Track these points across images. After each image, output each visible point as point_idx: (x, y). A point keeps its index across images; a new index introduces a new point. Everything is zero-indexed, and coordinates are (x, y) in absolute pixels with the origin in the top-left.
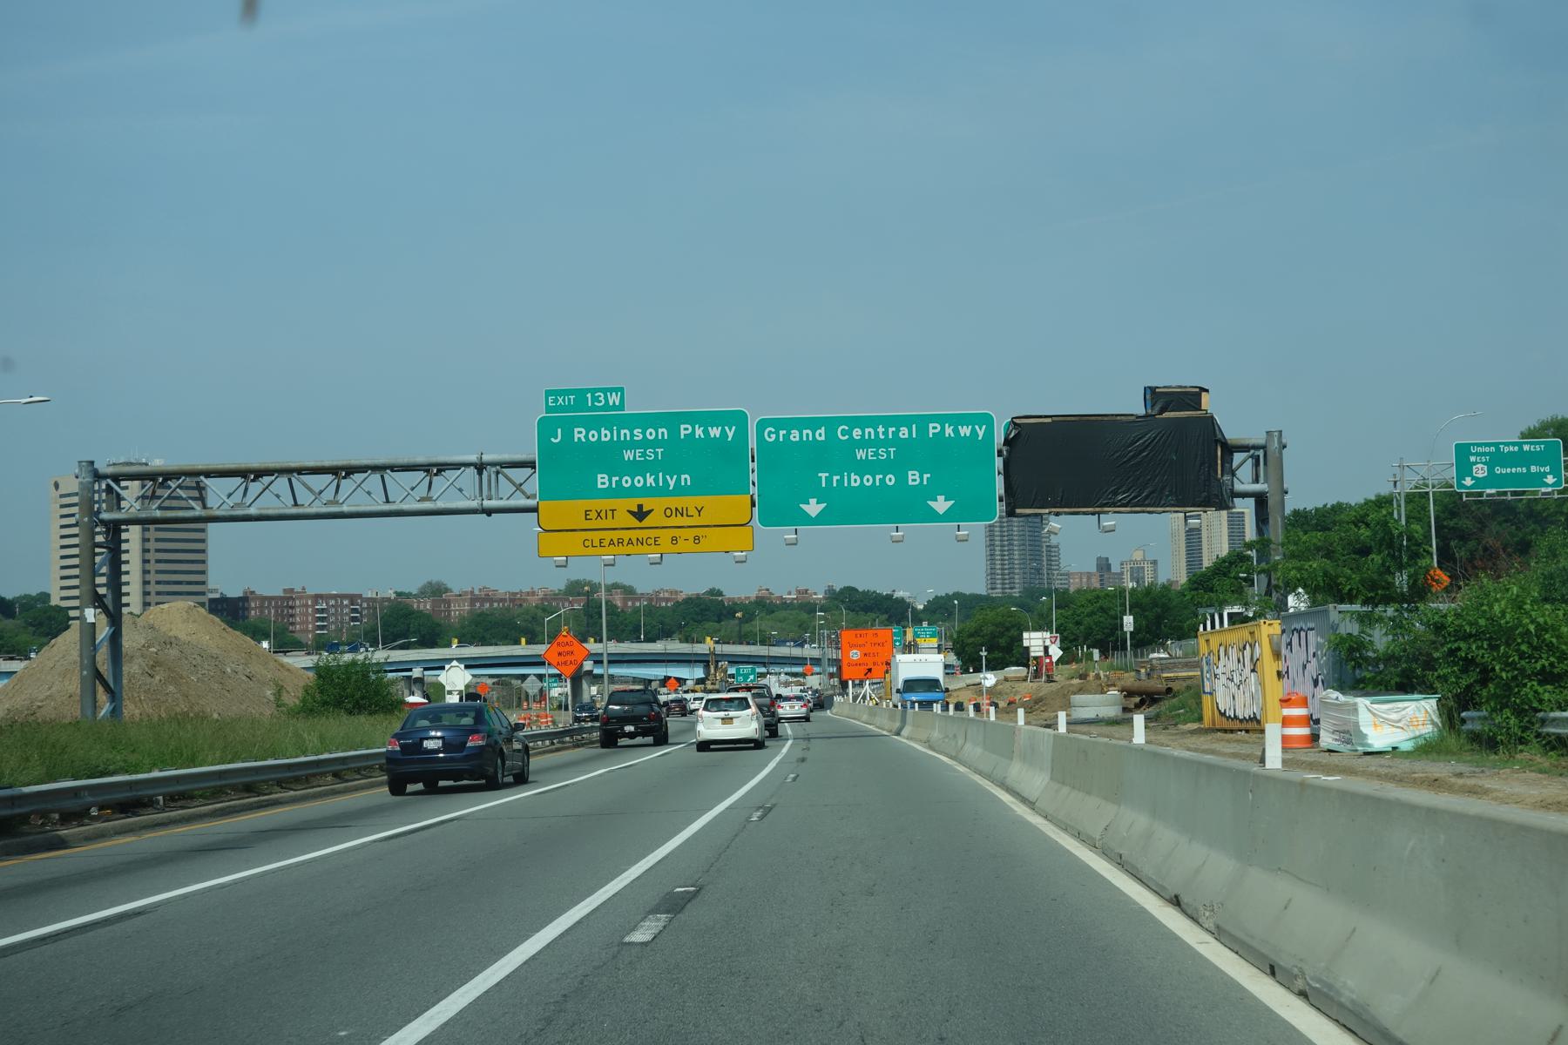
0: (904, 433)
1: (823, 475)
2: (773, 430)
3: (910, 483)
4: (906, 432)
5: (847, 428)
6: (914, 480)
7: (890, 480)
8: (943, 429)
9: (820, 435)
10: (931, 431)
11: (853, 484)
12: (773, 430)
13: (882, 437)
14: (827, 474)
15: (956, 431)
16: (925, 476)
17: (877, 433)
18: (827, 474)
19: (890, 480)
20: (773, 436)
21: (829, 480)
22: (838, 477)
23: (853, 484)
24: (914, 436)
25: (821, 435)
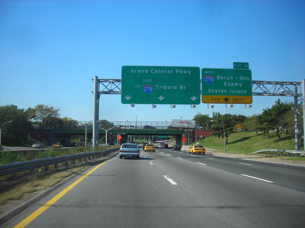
0: (169, 72)
1: (157, 86)
2: (133, 70)
3: (181, 89)
4: (170, 71)
5: (153, 70)
6: (182, 88)
7: (175, 88)
8: (179, 71)
9: (146, 71)
10: (176, 72)
11: (165, 88)
12: (133, 70)
13: (163, 73)
14: (158, 86)
15: (183, 72)
16: (185, 87)
17: (162, 72)
18: (158, 86)
19: (175, 88)
20: (133, 71)
21: (159, 87)
22: (161, 87)
23: (165, 88)
24: (172, 73)
25: (146, 71)
